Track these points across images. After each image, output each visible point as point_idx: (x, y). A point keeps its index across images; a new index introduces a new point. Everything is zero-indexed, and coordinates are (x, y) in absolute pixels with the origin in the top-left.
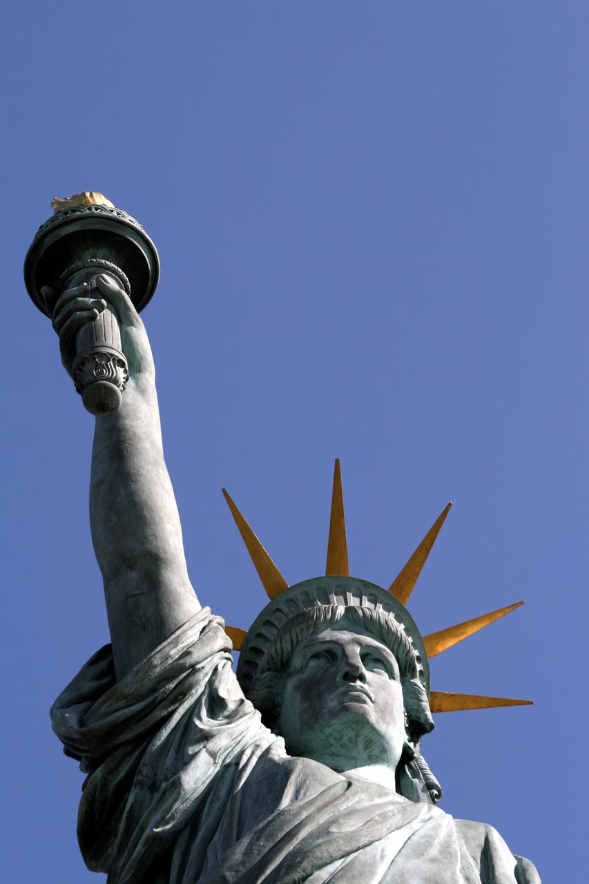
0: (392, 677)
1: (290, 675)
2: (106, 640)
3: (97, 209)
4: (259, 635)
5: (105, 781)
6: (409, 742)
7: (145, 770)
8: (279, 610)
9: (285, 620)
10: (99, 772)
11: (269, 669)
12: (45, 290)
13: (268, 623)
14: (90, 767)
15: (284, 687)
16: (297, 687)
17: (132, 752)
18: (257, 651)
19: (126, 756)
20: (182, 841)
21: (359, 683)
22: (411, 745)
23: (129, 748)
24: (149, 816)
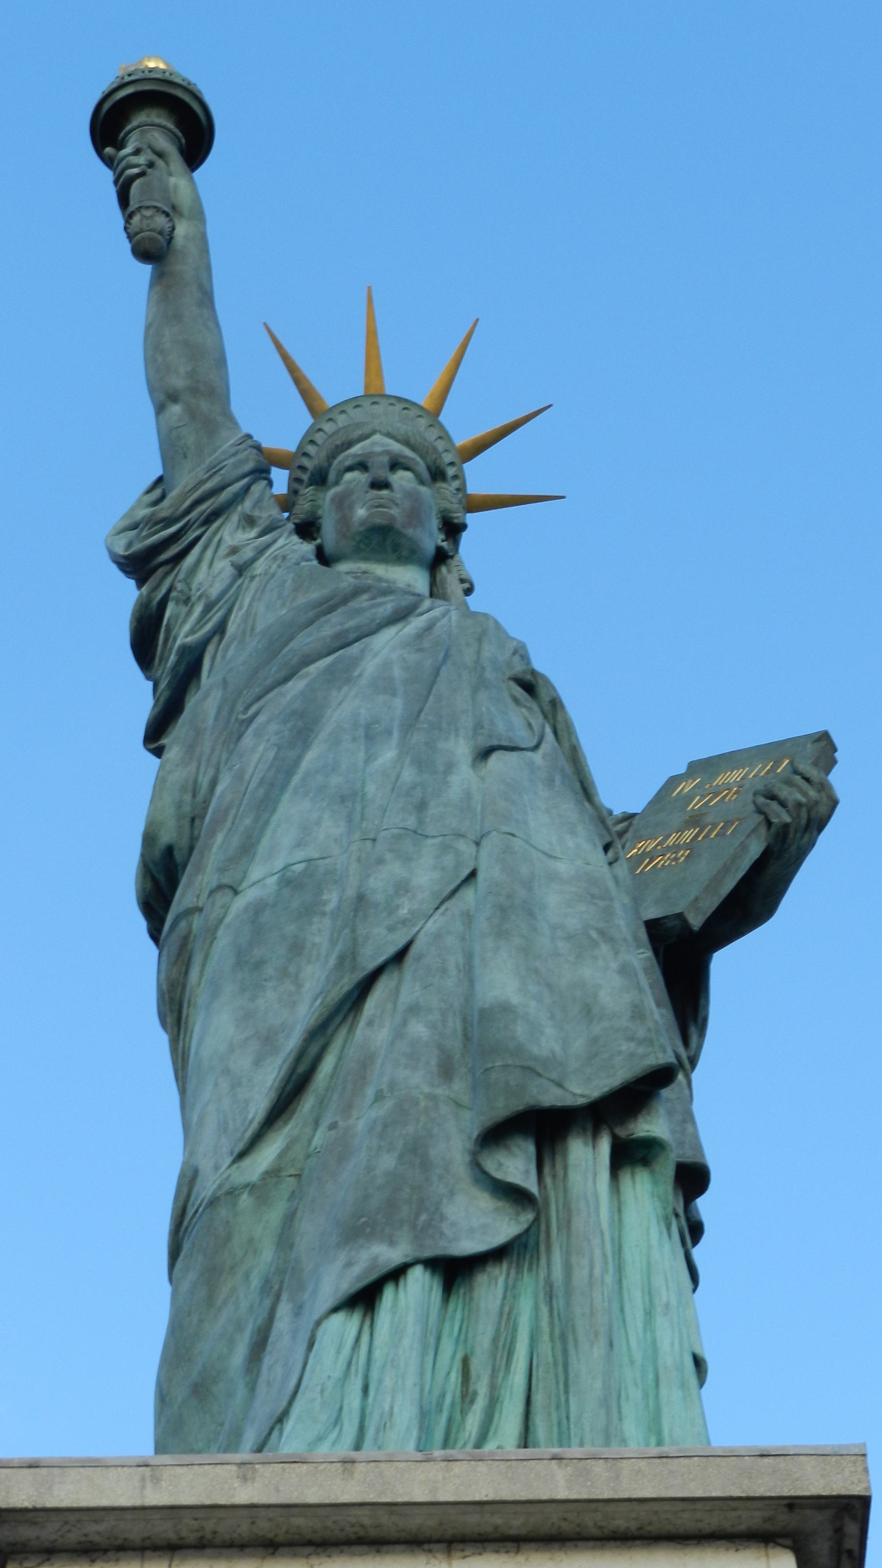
0: (422, 482)
1: (329, 488)
2: (159, 472)
3: (150, 71)
4: (305, 454)
5: (149, 599)
6: (443, 541)
7: (179, 586)
8: (320, 430)
9: (325, 437)
10: (144, 589)
11: (311, 485)
12: (109, 150)
13: (312, 442)
14: (140, 583)
15: (324, 499)
16: (333, 500)
17: (172, 570)
18: (302, 468)
19: (167, 574)
20: (210, 649)
21: (385, 492)
22: (445, 544)
23: (169, 567)
24: (180, 628)
